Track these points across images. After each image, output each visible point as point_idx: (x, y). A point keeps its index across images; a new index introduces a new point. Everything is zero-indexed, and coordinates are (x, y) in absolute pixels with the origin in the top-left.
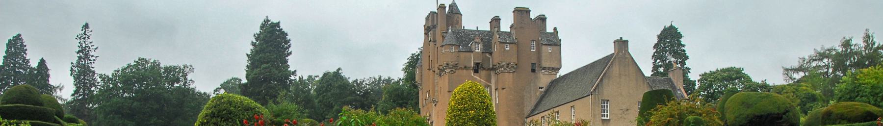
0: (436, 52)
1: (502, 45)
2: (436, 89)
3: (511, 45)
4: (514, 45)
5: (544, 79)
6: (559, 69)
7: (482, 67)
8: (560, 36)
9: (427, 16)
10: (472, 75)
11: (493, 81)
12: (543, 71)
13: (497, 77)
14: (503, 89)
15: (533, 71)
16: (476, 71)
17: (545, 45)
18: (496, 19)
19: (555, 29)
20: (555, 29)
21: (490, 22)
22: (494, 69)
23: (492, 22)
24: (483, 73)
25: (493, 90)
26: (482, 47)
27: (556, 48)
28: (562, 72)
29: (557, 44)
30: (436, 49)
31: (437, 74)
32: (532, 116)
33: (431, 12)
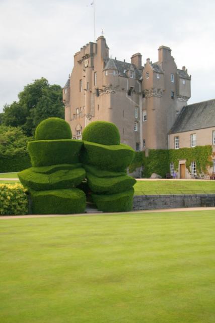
0: (93, 75)
1: (155, 73)
2: (92, 106)
3: (161, 75)
4: (162, 75)
5: (179, 105)
6: (189, 98)
7: (134, 91)
8: (189, 73)
9: (84, 46)
10: (127, 96)
11: (141, 103)
12: (179, 98)
13: (147, 100)
14: (154, 110)
15: (172, 97)
16: (129, 94)
17: (182, 78)
18: (139, 55)
19: (184, 68)
20: (184, 68)
21: (131, 58)
22: (140, 94)
23: (134, 58)
24: (134, 95)
25: (141, 110)
26: (135, 75)
27: (188, 81)
28: (190, 102)
29: (188, 79)
30: (93, 74)
31: (94, 94)
32: (185, 131)
33: (90, 42)
